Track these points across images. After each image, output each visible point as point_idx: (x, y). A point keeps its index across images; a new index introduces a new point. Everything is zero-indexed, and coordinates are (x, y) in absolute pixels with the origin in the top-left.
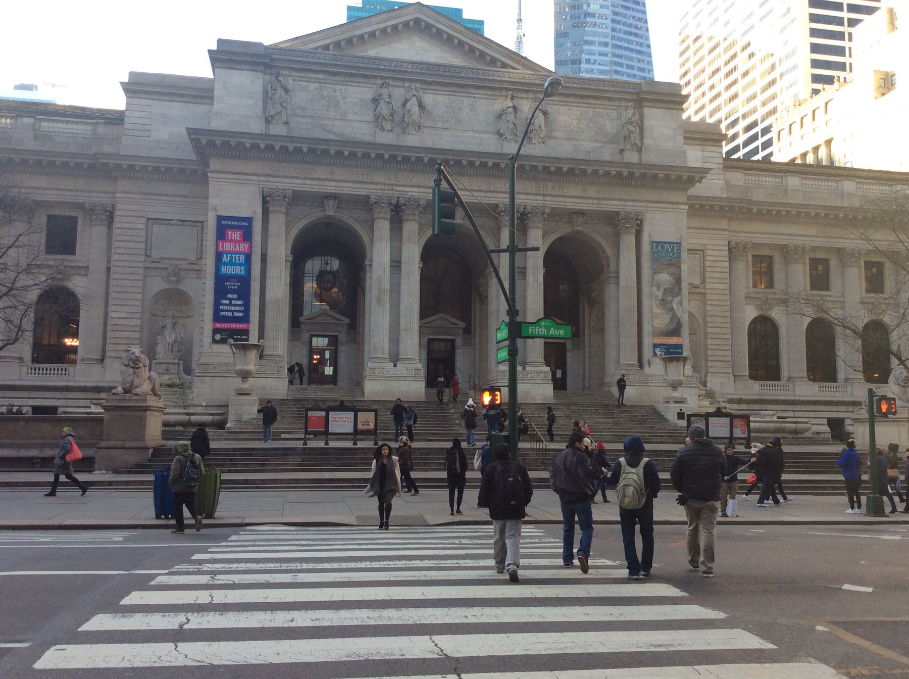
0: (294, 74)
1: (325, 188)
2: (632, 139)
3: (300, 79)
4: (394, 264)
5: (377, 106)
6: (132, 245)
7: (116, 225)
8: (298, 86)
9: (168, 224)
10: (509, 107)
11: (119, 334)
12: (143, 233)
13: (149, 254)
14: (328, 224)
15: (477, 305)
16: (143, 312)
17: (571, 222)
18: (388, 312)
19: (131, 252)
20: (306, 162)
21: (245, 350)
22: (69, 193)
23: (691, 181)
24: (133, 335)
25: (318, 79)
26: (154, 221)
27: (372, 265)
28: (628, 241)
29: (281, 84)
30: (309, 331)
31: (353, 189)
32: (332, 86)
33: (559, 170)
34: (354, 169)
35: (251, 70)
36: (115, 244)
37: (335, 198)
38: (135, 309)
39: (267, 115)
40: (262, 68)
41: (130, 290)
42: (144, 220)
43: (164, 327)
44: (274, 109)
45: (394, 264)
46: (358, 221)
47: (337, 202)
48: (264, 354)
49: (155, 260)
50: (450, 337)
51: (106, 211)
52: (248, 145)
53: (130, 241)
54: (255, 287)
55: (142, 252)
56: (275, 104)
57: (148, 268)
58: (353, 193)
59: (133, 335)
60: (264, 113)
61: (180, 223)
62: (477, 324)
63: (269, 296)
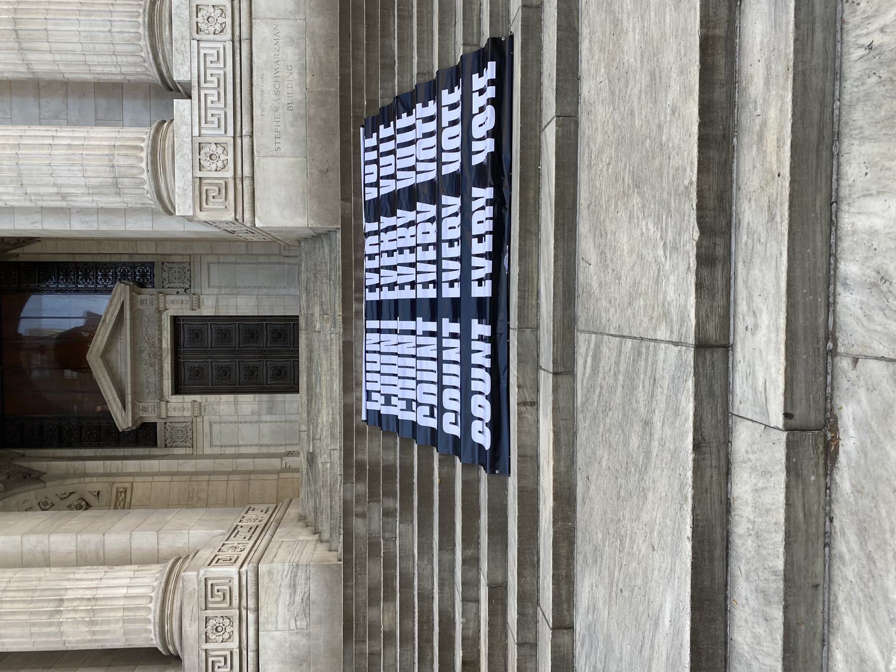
30: (161, 398)
48: (156, 643)
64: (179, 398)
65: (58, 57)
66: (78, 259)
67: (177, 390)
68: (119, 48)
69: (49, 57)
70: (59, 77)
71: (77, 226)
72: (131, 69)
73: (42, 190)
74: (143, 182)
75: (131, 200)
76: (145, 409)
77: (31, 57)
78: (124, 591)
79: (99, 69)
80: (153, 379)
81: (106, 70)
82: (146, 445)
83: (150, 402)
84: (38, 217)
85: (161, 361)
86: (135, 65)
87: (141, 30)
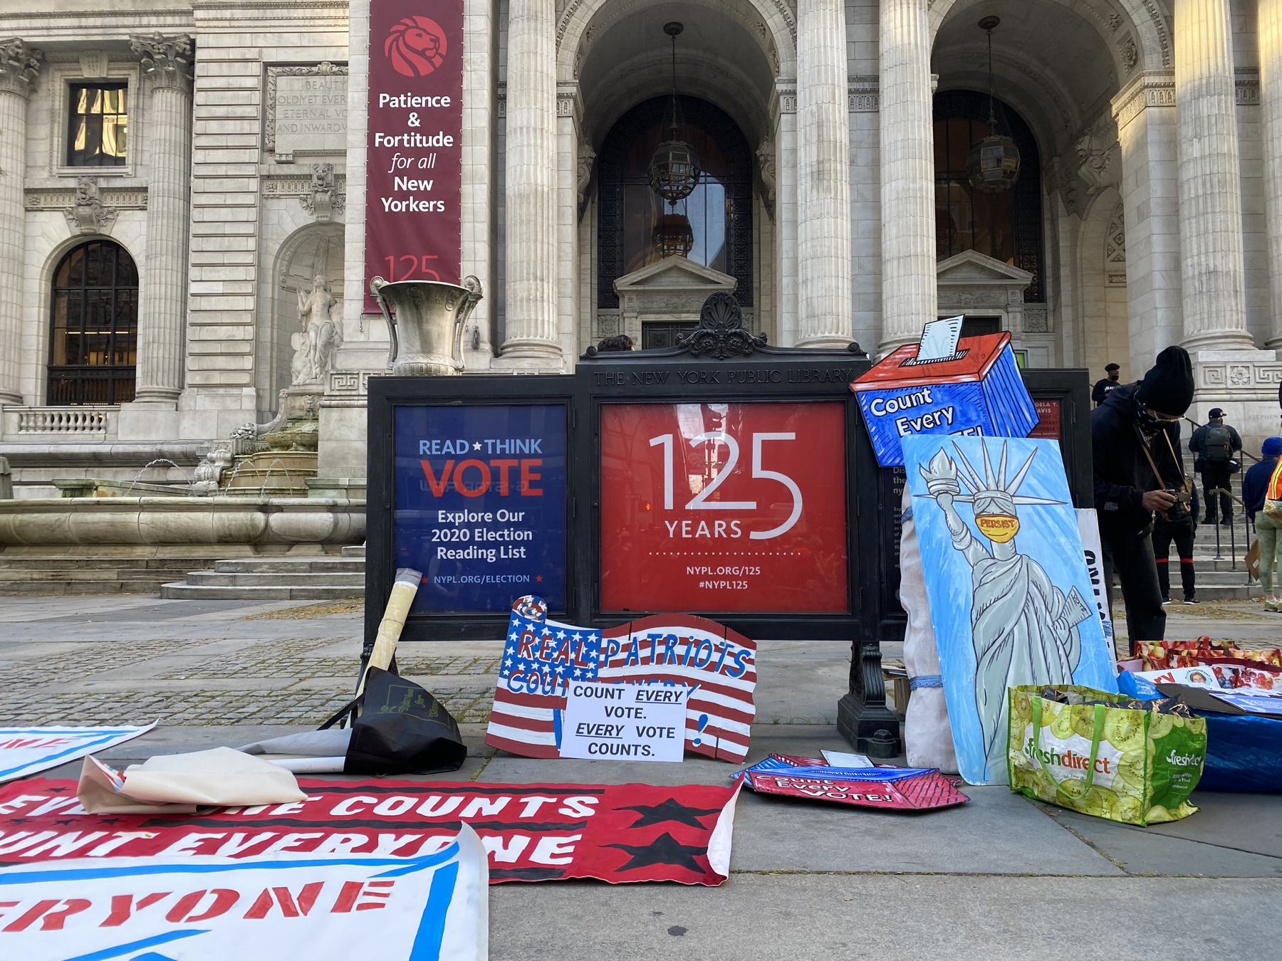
4: (856, 86)
6: (230, 126)
7: (199, 83)
9: (309, 74)
11: (206, 333)
12: (256, 97)
13: (271, 145)
14: (673, 29)
15: (1064, 226)
16: (260, 280)
18: (846, 208)
19: (232, 141)
21: (417, 307)
22: (98, 21)
24: (239, 333)
26: (279, 69)
27: (794, 93)
30: (641, 313)
36: (198, 127)
38: (240, 273)
41: (228, 229)
42: (256, 68)
43: (308, 314)
45: (856, 86)
49: (284, 158)
50: (991, 313)
51: (178, 54)
53: (228, 118)
54: (475, 158)
55: (254, 141)
57: (269, 177)
59: (239, 333)
61: (335, 69)
62: (1064, 272)
63: (513, 184)
64: (640, 327)
65: (895, 280)
66: (755, 246)
67: (644, 324)
68: (902, 318)
69: (895, 274)
70: (884, 278)
71: (785, 282)
72: (890, 325)
73: (809, 269)
74: (816, 333)
75: (803, 323)
76: (630, 300)
77: (895, 263)
78: (546, 319)
79: (889, 305)
80: (655, 306)
81: (889, 309)
82: (599, 300)
83: (636, 304)
84: (791, 255)
85: (671, 312)
86: (893, 327)
87: (914, 333)
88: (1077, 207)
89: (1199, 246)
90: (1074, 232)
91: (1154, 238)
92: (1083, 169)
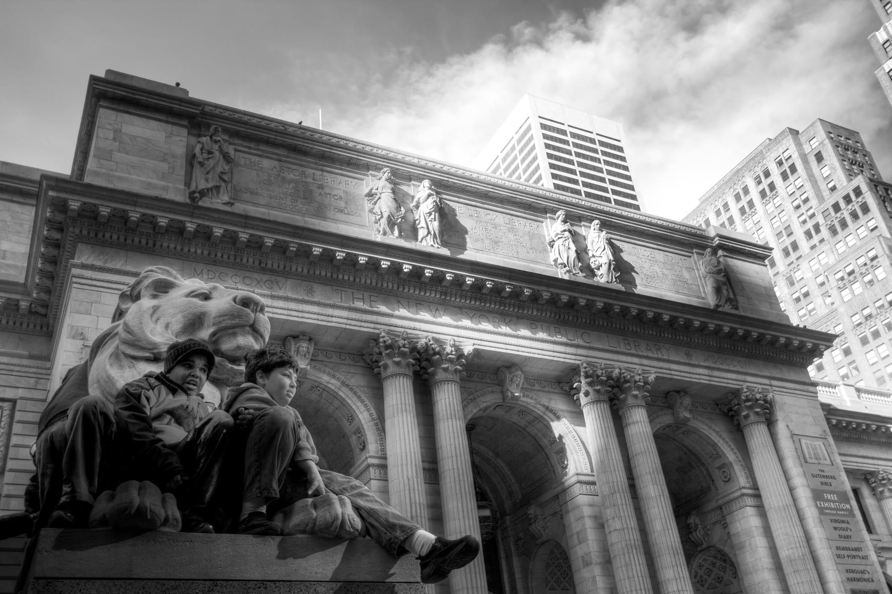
0: (237, 141)
1: (300, 314)
2: (724, 291)
3: (246, 150)
5: (375, 203)
8: (243, 159)
10: (565, 231)
15: (516, 563)
17: (671, 407)
20: (264, 270)
23: (816, 352)
25: (278, 155)
28: (757, 436)
29: (220, 147)
31: (349, 322)
32: (302, 169)
33: (657, 317)
34: (348, 290)
35: (167, 122)
37: (310, 339)
39: (193, 188)
40: (185, 123)
44: (207, 180)
46: (347, 386)
47: (313, 346)
52: (163, 222)
56: (208, 173)
58: (348, 327)
60: (188, 184)
88: (527, 554)
89: (630, 586)
90: (525, 571)
91: (598, 578)
92: (533, 526)
